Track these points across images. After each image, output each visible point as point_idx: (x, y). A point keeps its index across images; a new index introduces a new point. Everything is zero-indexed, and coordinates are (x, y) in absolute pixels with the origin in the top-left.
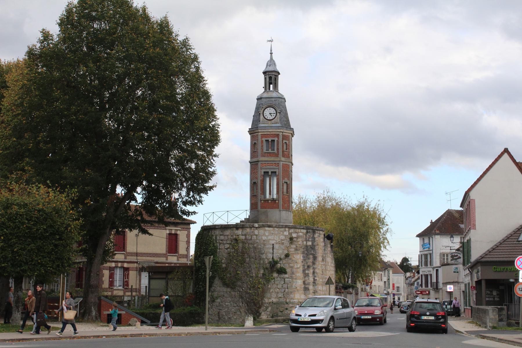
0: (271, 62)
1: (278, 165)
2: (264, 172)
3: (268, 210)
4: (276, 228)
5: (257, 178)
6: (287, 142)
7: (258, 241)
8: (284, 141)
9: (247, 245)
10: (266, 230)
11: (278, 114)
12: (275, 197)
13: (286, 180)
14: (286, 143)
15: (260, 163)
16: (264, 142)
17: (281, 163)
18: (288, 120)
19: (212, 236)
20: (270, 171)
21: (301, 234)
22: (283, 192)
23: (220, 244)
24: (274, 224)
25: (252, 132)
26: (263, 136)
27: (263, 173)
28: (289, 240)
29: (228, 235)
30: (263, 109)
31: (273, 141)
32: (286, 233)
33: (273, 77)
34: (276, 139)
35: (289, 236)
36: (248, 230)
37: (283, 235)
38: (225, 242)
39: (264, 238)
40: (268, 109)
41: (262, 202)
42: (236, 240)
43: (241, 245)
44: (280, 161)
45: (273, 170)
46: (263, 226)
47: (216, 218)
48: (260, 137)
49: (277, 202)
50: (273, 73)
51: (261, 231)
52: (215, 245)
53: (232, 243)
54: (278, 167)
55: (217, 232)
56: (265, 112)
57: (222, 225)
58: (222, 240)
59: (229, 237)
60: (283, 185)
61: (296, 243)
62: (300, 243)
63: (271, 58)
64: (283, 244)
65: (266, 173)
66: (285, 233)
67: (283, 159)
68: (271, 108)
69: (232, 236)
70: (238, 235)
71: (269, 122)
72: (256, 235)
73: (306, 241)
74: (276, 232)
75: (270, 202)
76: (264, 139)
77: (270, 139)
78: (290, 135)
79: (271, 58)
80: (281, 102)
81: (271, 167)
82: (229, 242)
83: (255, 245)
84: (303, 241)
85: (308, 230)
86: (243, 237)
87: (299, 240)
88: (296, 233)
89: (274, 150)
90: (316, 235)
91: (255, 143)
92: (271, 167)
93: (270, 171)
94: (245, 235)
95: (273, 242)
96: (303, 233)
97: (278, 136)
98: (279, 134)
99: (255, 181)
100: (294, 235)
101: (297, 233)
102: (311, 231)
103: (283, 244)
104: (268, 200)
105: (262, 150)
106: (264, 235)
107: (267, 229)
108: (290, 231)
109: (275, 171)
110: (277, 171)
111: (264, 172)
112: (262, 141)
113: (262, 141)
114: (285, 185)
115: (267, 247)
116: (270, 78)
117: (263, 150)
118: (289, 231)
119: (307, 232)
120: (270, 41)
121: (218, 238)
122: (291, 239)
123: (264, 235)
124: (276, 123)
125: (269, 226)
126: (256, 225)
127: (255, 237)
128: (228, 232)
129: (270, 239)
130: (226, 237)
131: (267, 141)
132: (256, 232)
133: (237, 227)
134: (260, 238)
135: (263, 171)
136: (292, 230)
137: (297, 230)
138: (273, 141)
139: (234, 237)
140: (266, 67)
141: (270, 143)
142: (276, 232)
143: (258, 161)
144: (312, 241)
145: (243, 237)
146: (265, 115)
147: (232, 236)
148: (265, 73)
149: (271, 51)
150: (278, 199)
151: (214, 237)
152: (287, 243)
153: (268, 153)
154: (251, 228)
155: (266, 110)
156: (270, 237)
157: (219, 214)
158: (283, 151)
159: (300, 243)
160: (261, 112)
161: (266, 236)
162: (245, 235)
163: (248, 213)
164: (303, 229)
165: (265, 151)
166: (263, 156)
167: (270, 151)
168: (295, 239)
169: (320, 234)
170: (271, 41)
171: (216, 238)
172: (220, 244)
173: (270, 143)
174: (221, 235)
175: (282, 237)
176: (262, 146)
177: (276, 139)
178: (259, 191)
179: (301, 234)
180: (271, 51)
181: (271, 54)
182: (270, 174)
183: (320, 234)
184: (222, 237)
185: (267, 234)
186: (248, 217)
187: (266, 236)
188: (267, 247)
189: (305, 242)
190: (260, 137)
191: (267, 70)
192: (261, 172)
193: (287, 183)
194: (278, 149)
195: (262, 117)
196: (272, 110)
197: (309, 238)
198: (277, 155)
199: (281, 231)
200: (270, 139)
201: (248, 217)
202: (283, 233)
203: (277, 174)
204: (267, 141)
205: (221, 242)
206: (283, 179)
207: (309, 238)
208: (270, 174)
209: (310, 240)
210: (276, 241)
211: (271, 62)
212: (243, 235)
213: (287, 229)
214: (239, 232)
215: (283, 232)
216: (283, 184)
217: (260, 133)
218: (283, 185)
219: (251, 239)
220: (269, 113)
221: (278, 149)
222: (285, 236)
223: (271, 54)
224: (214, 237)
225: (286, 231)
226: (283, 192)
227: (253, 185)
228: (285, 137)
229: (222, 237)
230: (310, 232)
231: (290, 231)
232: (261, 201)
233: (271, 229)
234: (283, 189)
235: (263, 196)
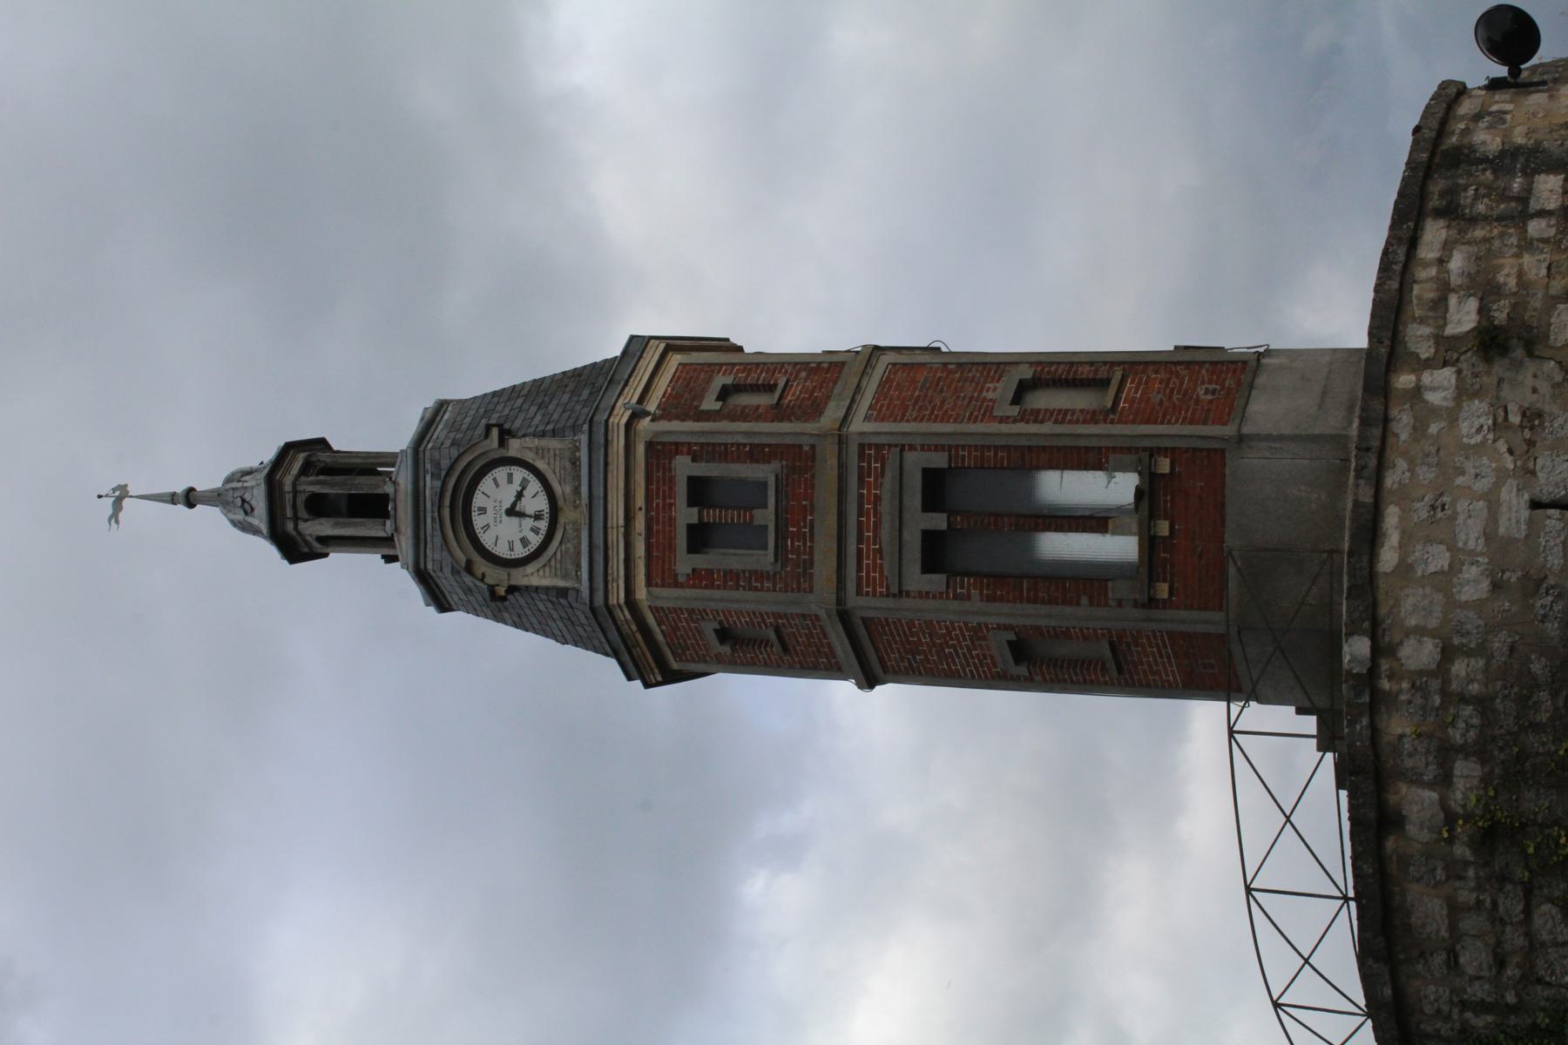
0: (230, 498)
1: (871, 450)
2: (929, 566)
3: (1232, 540)
4: (1391, 480)
5: (978, 632)
6: (720, 380)
7: (1499, 643)
8: (710, 403)
9: (1533, 741)
10: (1404, 569)
11: (515, 447)
12: (1120, 488)
13: (1000, 391)
14: (724, 393)
15: (853, 600)
16: (701, 561)
17: (858, 425)
18: (577, 374)
19: (1465, 1030)
20: (922, 522)
21: (1457, 263)
22: (1092, 417)
23: (1529, 978)
24: (1357, 492)
25: (655, 659)
26: (660, 573)
27: (937, 581)
28: (1499, 368)
29: (1454, 909)
30: (481, 566)
31: (699, 491)
32: (1440, 384)
33: (311, 486)
34: (684, 467)
35: (1469, 360)
36: (1398, 726)
37: (1453, 416)
38: (1514, 939)
39: (1473, 585)
40: (478, 521)
41: (1163, 590)
42: (1490, 837)
43: (1537, 802)
44: (842, 441)
45: (914, 500)
46: (1366, 585)
47: (1308, 990)
48: (669, 596)
49: (1164, 466)
50: (288, 482)
51: (1412, 607)
52: (1543, 1020)
53: (1521, 873)
54: (892, 457)
55: (1430, 993)
56: (502, 551)
57: (1367, 955)
58: (1500, 963)
59: (1466, 896)
60: (1036, 416)
61: (1537, 302)
62: (1535, 266)
63: (216, 498)
64: (1532, 417)
65: (935, 552)
66: (1434, 398)
67: (833, 413)
68: (478, 500)
69: (1455, 871)
70: (1450, 819)
71: (567, 516)
72: (1448, 652)
73: (1524, 216)
74: (1426, 474)
75: (1163, 528)
76: (684, 563)
77: (685, 515)
78: (675, 360)
79: (216, 498)
80: (453, 426)
81: (886, 507)
82: (1511, 905)
83: (1537, 667)
84: (1527, 245)
85: (1434, 202)
86: (1466, 772)
87: (1507, 276)
88: (1439, 305)
89: (763, 485)
90: (1487, 140)
91: (724, 634)
92: (886, 507)
93: (922, 522)
94: (1446, 753)
95: (1514, 503)
96: (1448, 246)
97: (660, 452)
98: (650, 445)
99: (998, 646)
100: (1463, 317)
101: (1445, 289)
102: (1437, 186)
103: (1532, 417)
104: (1150, 544)
105: (755, 579)
106: (1444, 581)
107: (1388, 558)
108: (1425, 351)
109: (915, 483)
110: (916, 462)
111: (929, 566)
112: (699, 578)
113: (699, 578)
114: (1043, 400)
115: (1555, 561)
116: (318, 506)
117: (760, 576)
118: (1428, 364)
119: (1450, 212)
120: (118, 505)
121: (1479, 991)
122: (1491, 342)
123: (1444, 581)
124: (575, 462)
125: (1369, 533)
126: (1357, 649)
127: (1459, 668)
128: (1426, 909)
129: (1489, 536)
130: (1469, 923)
131: (699, 538)
132: (1418, 654)
133: (1373, 828)
134: (1472, 621)
135: (916, 579)
136: (1419, 338)
137: (1422, 291)
138: (699, 491)
139: (1461, 851)
140: (255, 531)
141: (711, 515)
142: (1426, 474)
143: (844, 617)
144: (1530, 174)
145: (1466, 772)
146: (520, 552)
147: (1455, 871)
148: (294, 550)
149: (172, 499)
150: (1139, 456)
151: (1480, 1022)
152: (1530, 383)
153: (781, 535)
154: (1378, 703)
155: (487, 540)
156: (1470, 534)
157: (1281, 964)
158: (779, 412)
159: (1535, 266)
160: (494, 575)
161: (1454, 568)
162: (1446, 753)
163: (1256, 715)
164: (1413, 243)
165: (764, 559)
166: (797, 574)
167: (766, 516)
168: (1500, 315)
169: (1478, 117)
170: (120, 496)
171: (1482, 1007)
172: (1529, 978)
173: (711, 515)
174: (1453, 963)
175: (1475, 419)
176: (732, 578)
177: (684, 467)
178: (1078, 615)
179: (1457, 263)
180: (172, 499)
181: (190, 498)
182: (939, 521)
183: (1478, 117)
184: (1473, 957)
185: (1439, 559)
186: (1310, 724)
187: (1454, 568)
188: (1555, 561)
189: (1536, 228)
190: (669, 596)
191: (264, 528)
192: (926, 599)
193: (1023, 388)
194: (757, 453)
195: (532, 577)
196: (495, 492)
197: (1504, 197)
198: (798, 459)
199: (1419, 429)
200: (685, 515)
201: (1310, 724)
202: (1434, 412)
203: (939, 460)
204: (699, 538)
205: (1511, 971)
206: (988, 414)
207: (1504, 197)
208: (939, 521)
209: (1517, 185)
210: (1502, 476)
211: (230, 498)
212: (1444, 780)
213: (1404, 380)
214: (1418, 804)
215: (1426, 413)
216: (1023, 418)
217: (641, 593)
218: (1036, 416)
219: (1483, 704)
220: (505, 515)
221: (757, 453)
222: (1463, 393)
223: (190, 498)
224: (1480, 1022)
225: (1418, 390)
226: (1092, 417)
227: (1033, 663)
228: (680, 404)
229: (1473, 957)
230: (1451, 193)
231: (1425, 351)
232: (1152, 602)
233: (1392, 517)
234: (1062, 416)
235: (1118, 590)
